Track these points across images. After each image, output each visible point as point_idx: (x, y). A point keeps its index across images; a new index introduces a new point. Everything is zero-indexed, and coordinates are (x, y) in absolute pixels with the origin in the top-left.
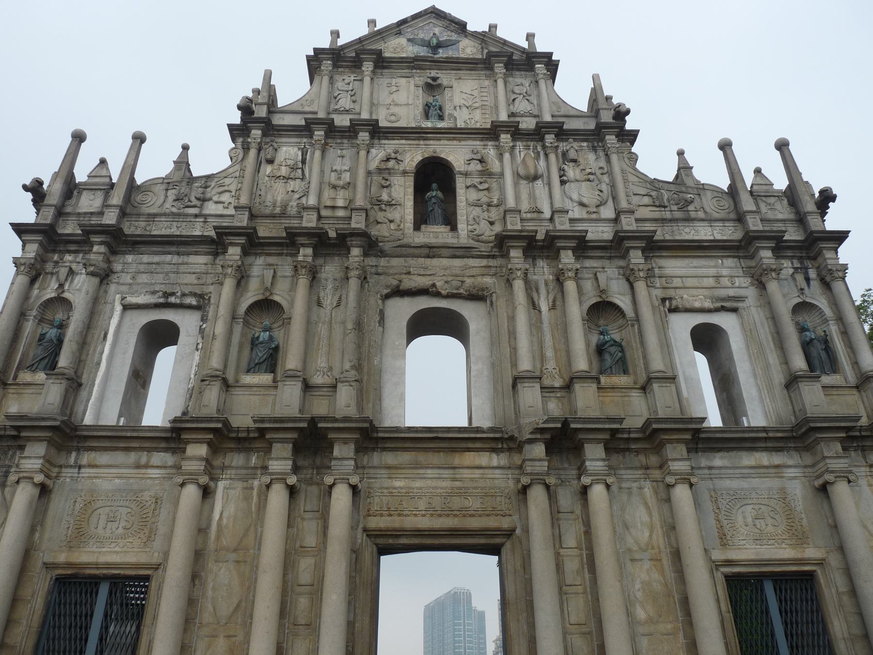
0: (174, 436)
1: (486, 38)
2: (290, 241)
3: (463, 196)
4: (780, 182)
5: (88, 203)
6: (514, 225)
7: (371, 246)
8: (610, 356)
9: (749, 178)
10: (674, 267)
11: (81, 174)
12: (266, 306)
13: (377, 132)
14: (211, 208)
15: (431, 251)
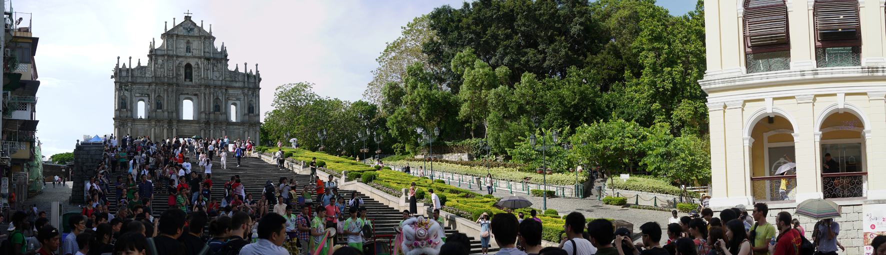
0: (149, 119)
1: (201, 29)
2: (163, 84)
3: (194, 74)
4: (254, 73)
5: (124, 74)
6: (203, 82)
7: (178, 85)
8: (217, 108)
9: (248, 71)
10: (231, 91)
11: (121, 66)
12: (159, 96)
13: (178, 57)
14: (147, 75)
15: (188, 86)
